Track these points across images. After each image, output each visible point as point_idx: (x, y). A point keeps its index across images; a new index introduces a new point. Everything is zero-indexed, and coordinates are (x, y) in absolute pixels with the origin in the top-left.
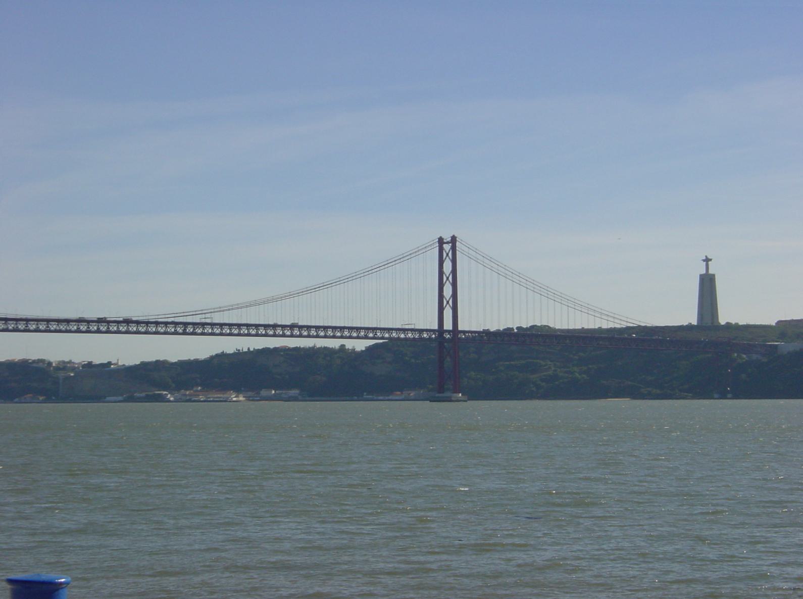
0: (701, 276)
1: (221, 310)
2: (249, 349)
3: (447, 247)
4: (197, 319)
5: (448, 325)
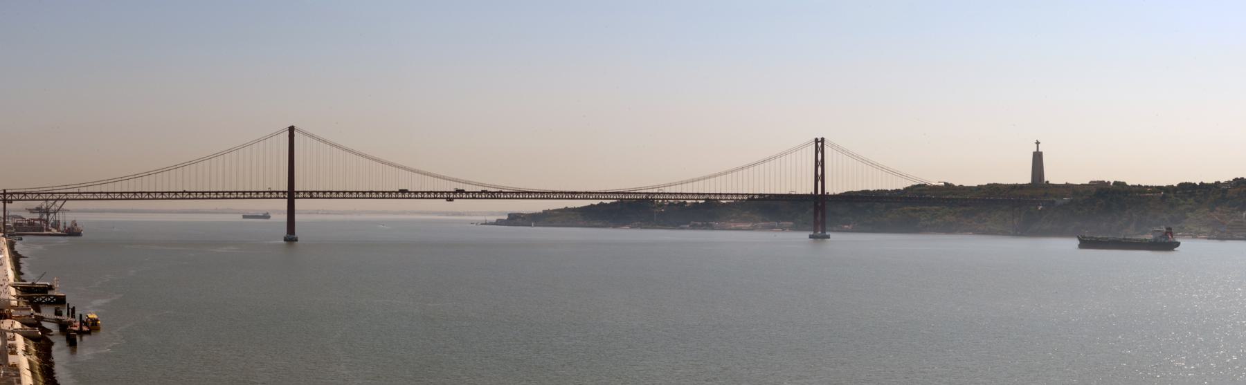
0: (1034, 153)
3: (820, 144)
4: (655, 191)
5: (820, 193)
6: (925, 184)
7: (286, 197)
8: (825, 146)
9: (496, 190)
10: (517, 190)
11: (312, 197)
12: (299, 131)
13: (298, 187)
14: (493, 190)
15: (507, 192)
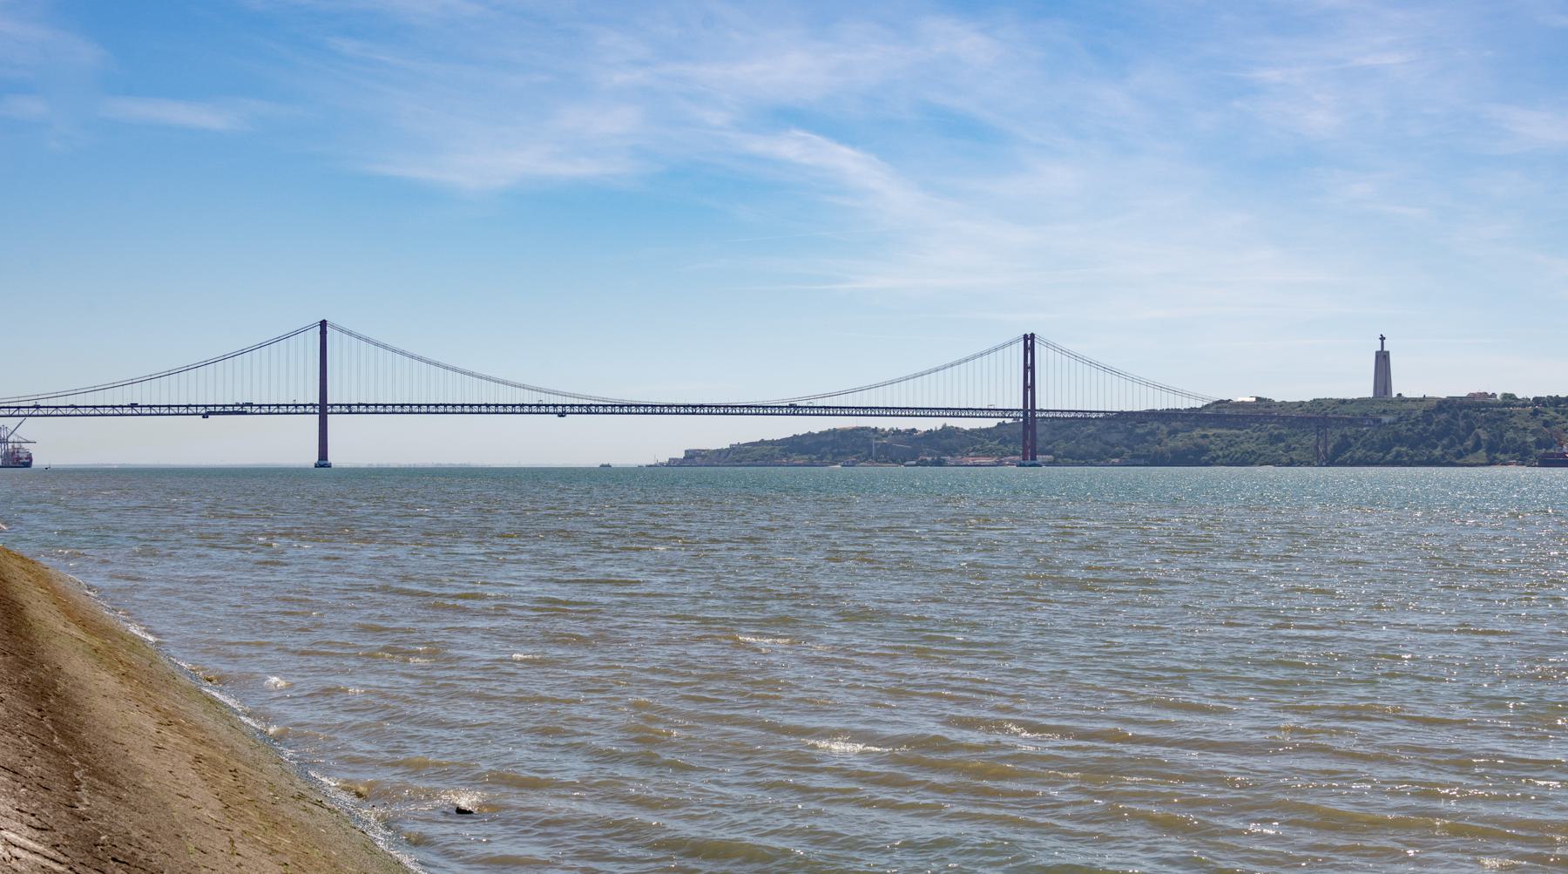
0: (1377, 352)
1: (816, 398)
2: (936, 428)
3: (1029, 341)
5: (1029, 408)
6: (1314, 400)
7: (317, 411)
8: (1036, 345)
9: (593, 403)
11: (350, 413)
12: (333, 326)
14: (588, 402)
15: (607, 406)
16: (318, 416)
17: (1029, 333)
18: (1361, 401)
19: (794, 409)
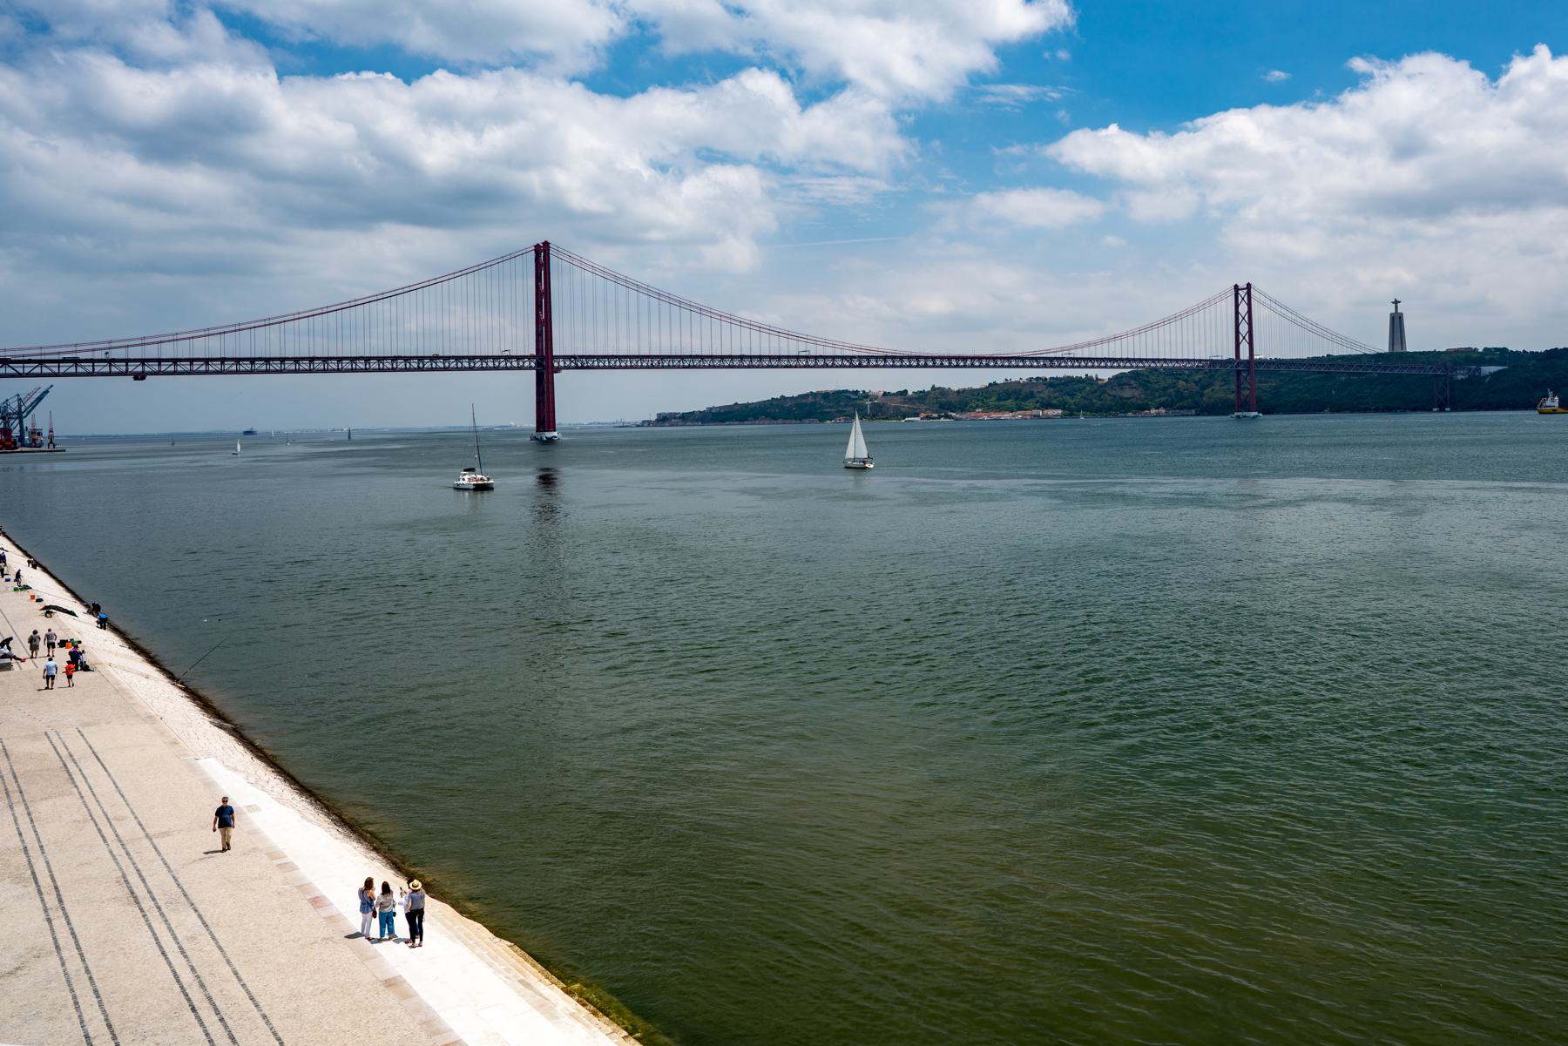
4: (1059, 355)
7: (533, 365)
10: (910, 354)
13: (562, 345)
16: (534, 372)
17: (1242, 284)
18: (1379, 356)
19: (1051, 362)
